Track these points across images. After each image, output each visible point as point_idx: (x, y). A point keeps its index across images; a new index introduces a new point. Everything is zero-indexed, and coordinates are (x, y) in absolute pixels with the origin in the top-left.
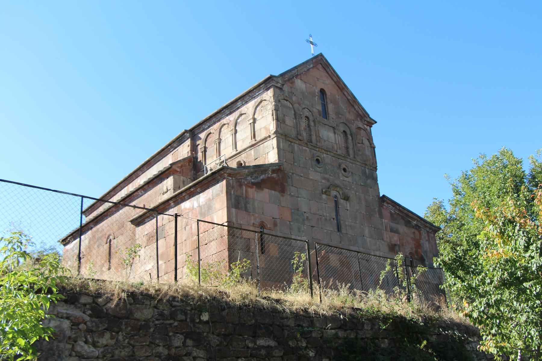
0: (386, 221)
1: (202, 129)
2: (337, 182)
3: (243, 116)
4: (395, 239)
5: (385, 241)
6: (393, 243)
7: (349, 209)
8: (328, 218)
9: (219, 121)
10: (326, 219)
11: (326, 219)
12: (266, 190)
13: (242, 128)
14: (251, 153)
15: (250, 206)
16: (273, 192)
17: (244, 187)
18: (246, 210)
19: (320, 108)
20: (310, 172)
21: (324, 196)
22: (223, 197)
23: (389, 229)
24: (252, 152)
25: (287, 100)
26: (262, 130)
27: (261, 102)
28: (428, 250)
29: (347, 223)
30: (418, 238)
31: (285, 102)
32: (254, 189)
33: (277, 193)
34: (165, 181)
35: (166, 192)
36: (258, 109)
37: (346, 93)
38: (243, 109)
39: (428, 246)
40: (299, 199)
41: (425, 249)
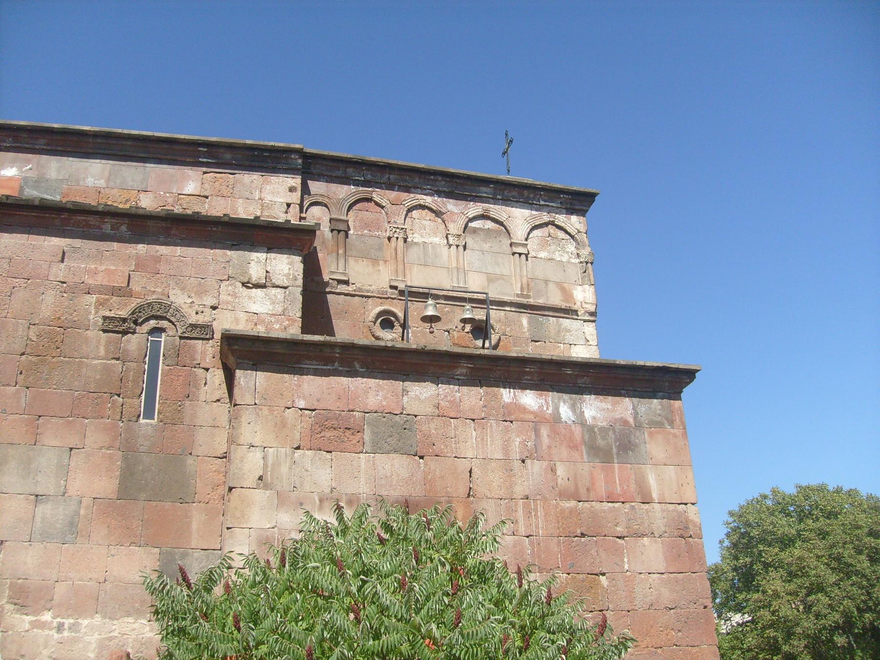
1: (339, 173)
3: (489, 225)
9: (407, 190)
13: (486, 246)
14: (521, 322)
22: (675, 436)
24: (524, 320)
26: (552, 287)
27: (546, 224)
34: (262, 256)
35: (257, 286)
36: (536, 232)
38: (498, 211)
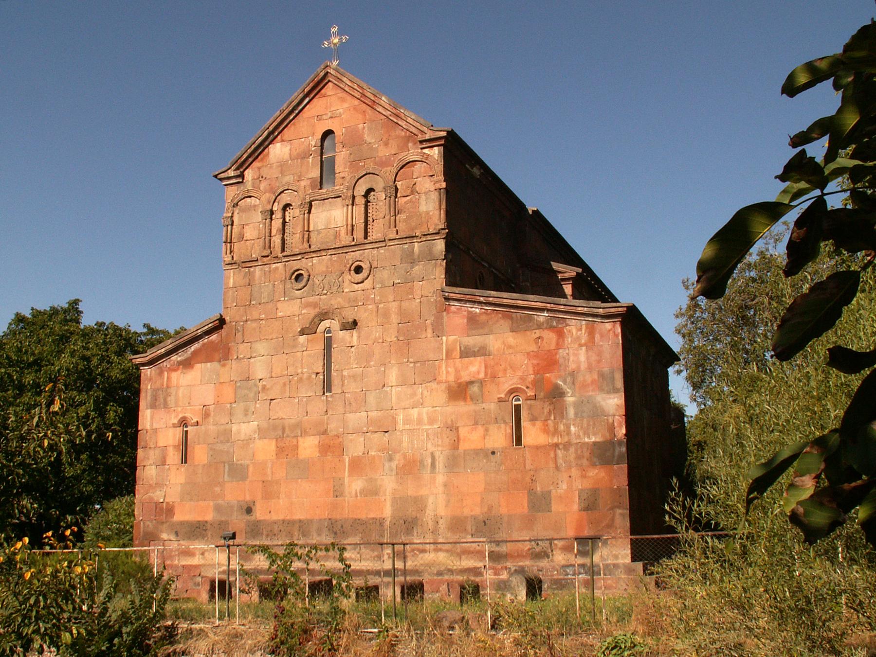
0: (452, 338)
2: (336, 301)
4: (475, 368)
5: (440, 382)
6: (465, 377)
7: (355, 343)
8: (305, 376)
10: (301, 380)
11: (301, 380)
12: (198, 366)
15: (171, 400)
16: (209, 364)
17: (166, 373)
18: (166, 406)
19: (316, 173)
20: (279, 305)
21: (302, 339)
23: (457, 353)
25: (250, 197)
28: (584, 366)
29: (345, 373)
30: (553, 347)
31: (248, 200)
32: (179, 372)
33: (215, 365)
37: (380, 109)
39: (582, 358)
40: (252, 360)
41: (572, 366)
